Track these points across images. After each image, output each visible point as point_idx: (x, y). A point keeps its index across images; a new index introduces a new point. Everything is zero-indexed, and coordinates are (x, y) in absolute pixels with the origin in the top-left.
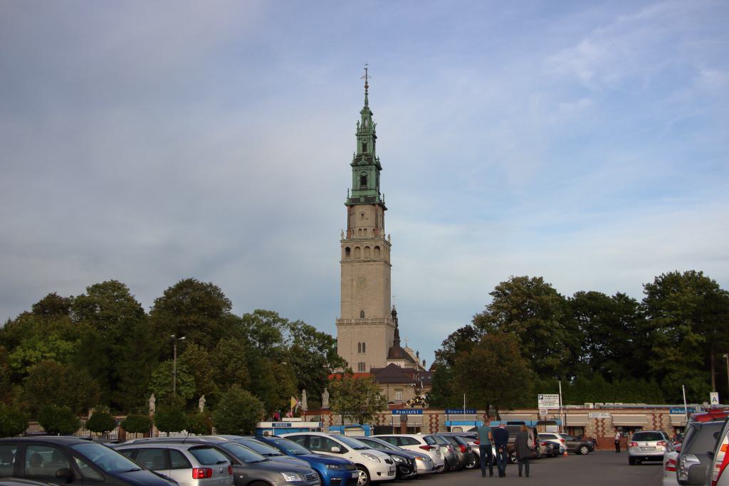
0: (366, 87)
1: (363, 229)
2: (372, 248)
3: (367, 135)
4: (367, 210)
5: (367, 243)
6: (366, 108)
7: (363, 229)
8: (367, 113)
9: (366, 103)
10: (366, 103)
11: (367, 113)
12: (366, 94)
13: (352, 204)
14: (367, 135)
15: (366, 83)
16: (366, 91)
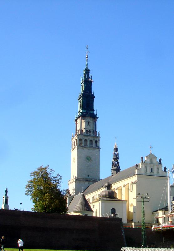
0: (87, 57)
1: (88, 130)
2: (94, 142)
3: (88, 83)
4: (90, 120)
5: (92, 139)
6: (87, 68)
7: (88, 130)
8: (87, 71)
9: (87, 66)
10: (87, 66)
11: (87, 71)
12: (87, 61)
13: (83, 116)
14: (88, 83)
15: (87, 55)
16: (87, 59)
